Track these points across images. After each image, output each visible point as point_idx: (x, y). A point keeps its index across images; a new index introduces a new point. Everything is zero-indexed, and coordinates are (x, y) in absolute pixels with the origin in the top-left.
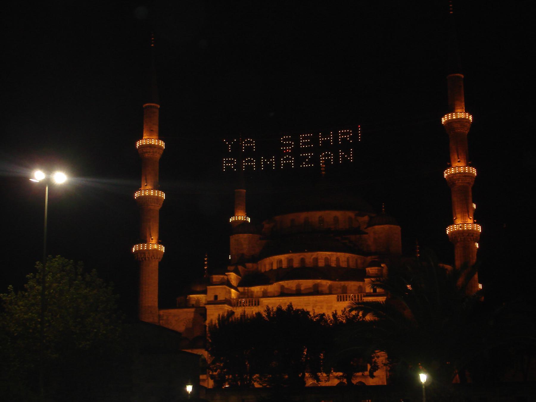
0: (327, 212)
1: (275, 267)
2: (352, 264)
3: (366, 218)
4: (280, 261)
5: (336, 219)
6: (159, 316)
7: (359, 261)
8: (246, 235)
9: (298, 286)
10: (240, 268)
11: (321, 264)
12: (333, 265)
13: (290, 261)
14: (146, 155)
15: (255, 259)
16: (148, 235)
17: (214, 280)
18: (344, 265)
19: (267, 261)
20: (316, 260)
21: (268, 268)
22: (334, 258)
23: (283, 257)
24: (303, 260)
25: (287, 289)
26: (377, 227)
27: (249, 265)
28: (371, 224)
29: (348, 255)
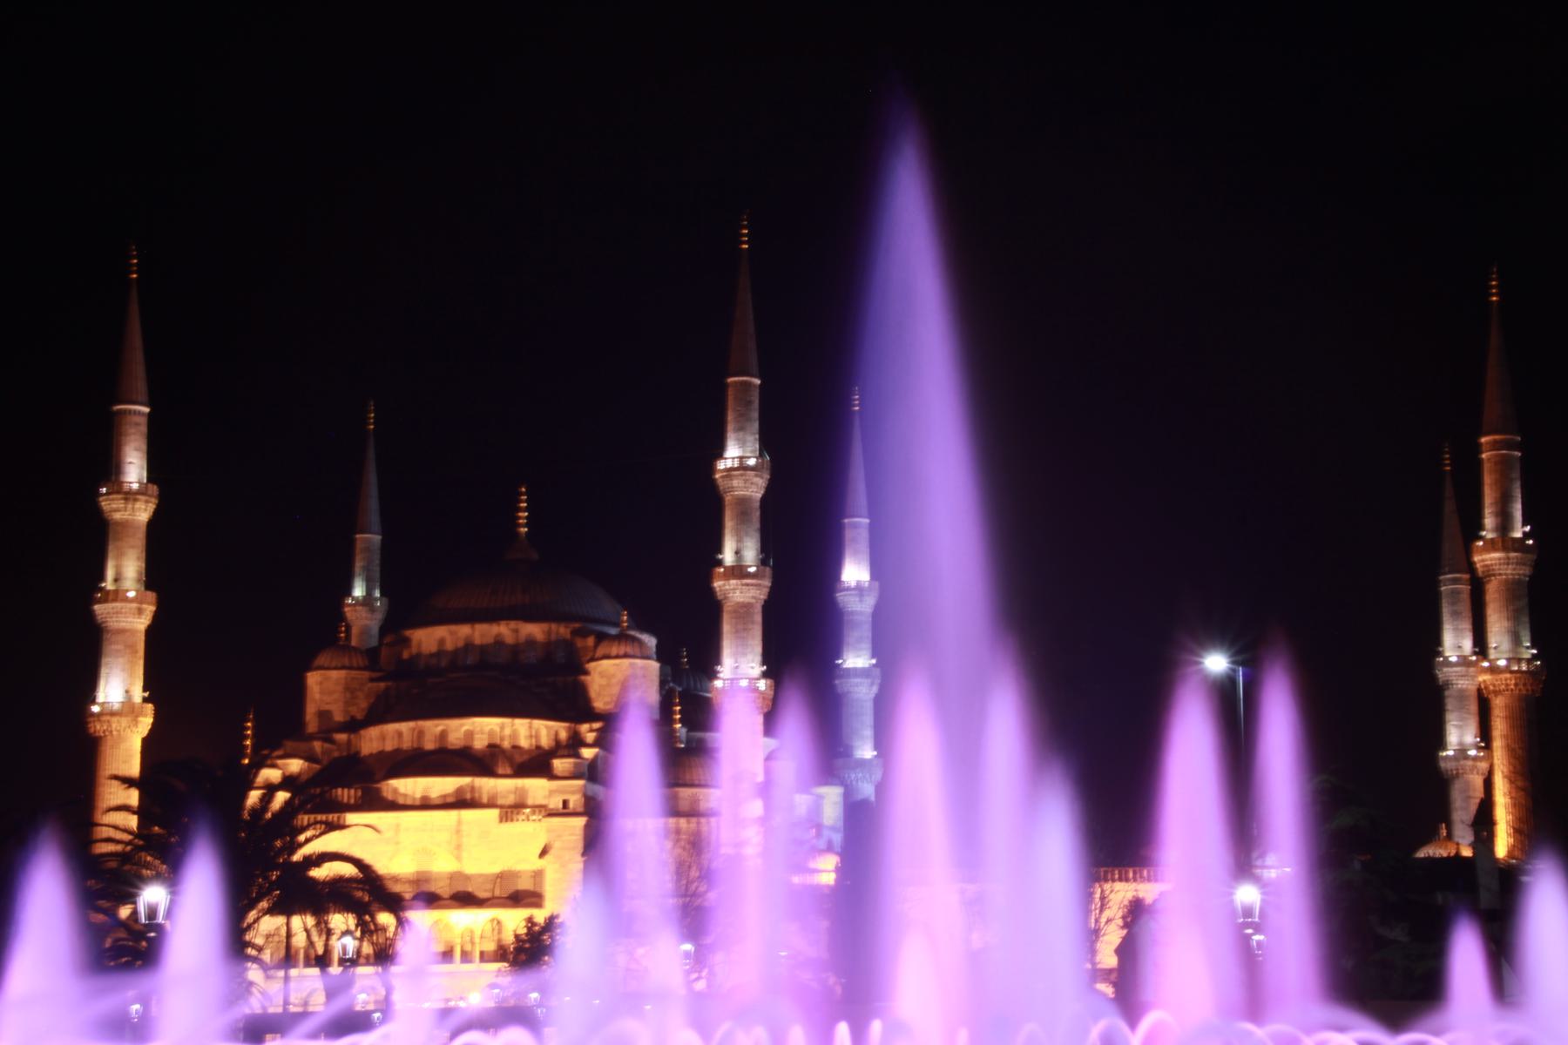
0: (513, 624)
1: (389, 747)
3: (590, 641)
4: (400, 734)
7: (563, 735)
8: (335, 674)
10: (317, 746)
11: (479, 743)
12: (506, 744)
14: (117, 516)
15: (354, 726)
18: (524, 743)
19: (373, 732)
23: (405, 727)
25: (405, 795)
26: (605, 662)
27: (342, 737)
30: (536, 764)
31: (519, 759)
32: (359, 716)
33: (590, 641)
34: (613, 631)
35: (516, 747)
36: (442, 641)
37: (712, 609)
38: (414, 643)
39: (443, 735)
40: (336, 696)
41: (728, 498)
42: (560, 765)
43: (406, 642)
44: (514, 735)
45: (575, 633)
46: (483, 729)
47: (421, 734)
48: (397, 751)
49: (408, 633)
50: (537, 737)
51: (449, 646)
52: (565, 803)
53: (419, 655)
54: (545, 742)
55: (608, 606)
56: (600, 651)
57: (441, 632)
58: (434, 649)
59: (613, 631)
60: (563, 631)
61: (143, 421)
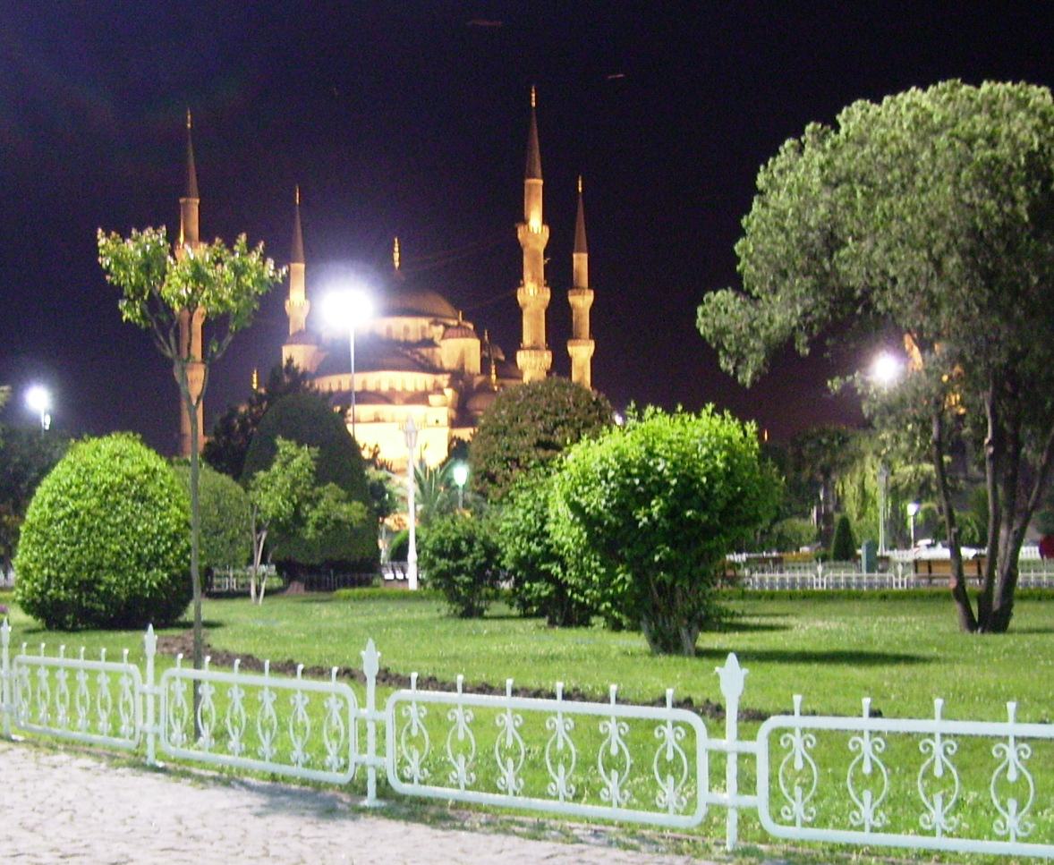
3: (441, 329)
5: (406, 330)
11: (384, 388)
12: (398, 388)
24: (364, 382)
28: (443, 337)
30: (421, 398)
31: (407, 396)
33: (441, 329)
34: (454, 323)
35: (404, 390)
37: (516, 312)
39: (364, 382)
41: (526, 250)
42: (433, 399)
45: (431, 324)
50: (415, 384)
54: (421, 388)
55: (444, 307)
56: (447, 334)
59: (454, 323)
60: (424, 322)
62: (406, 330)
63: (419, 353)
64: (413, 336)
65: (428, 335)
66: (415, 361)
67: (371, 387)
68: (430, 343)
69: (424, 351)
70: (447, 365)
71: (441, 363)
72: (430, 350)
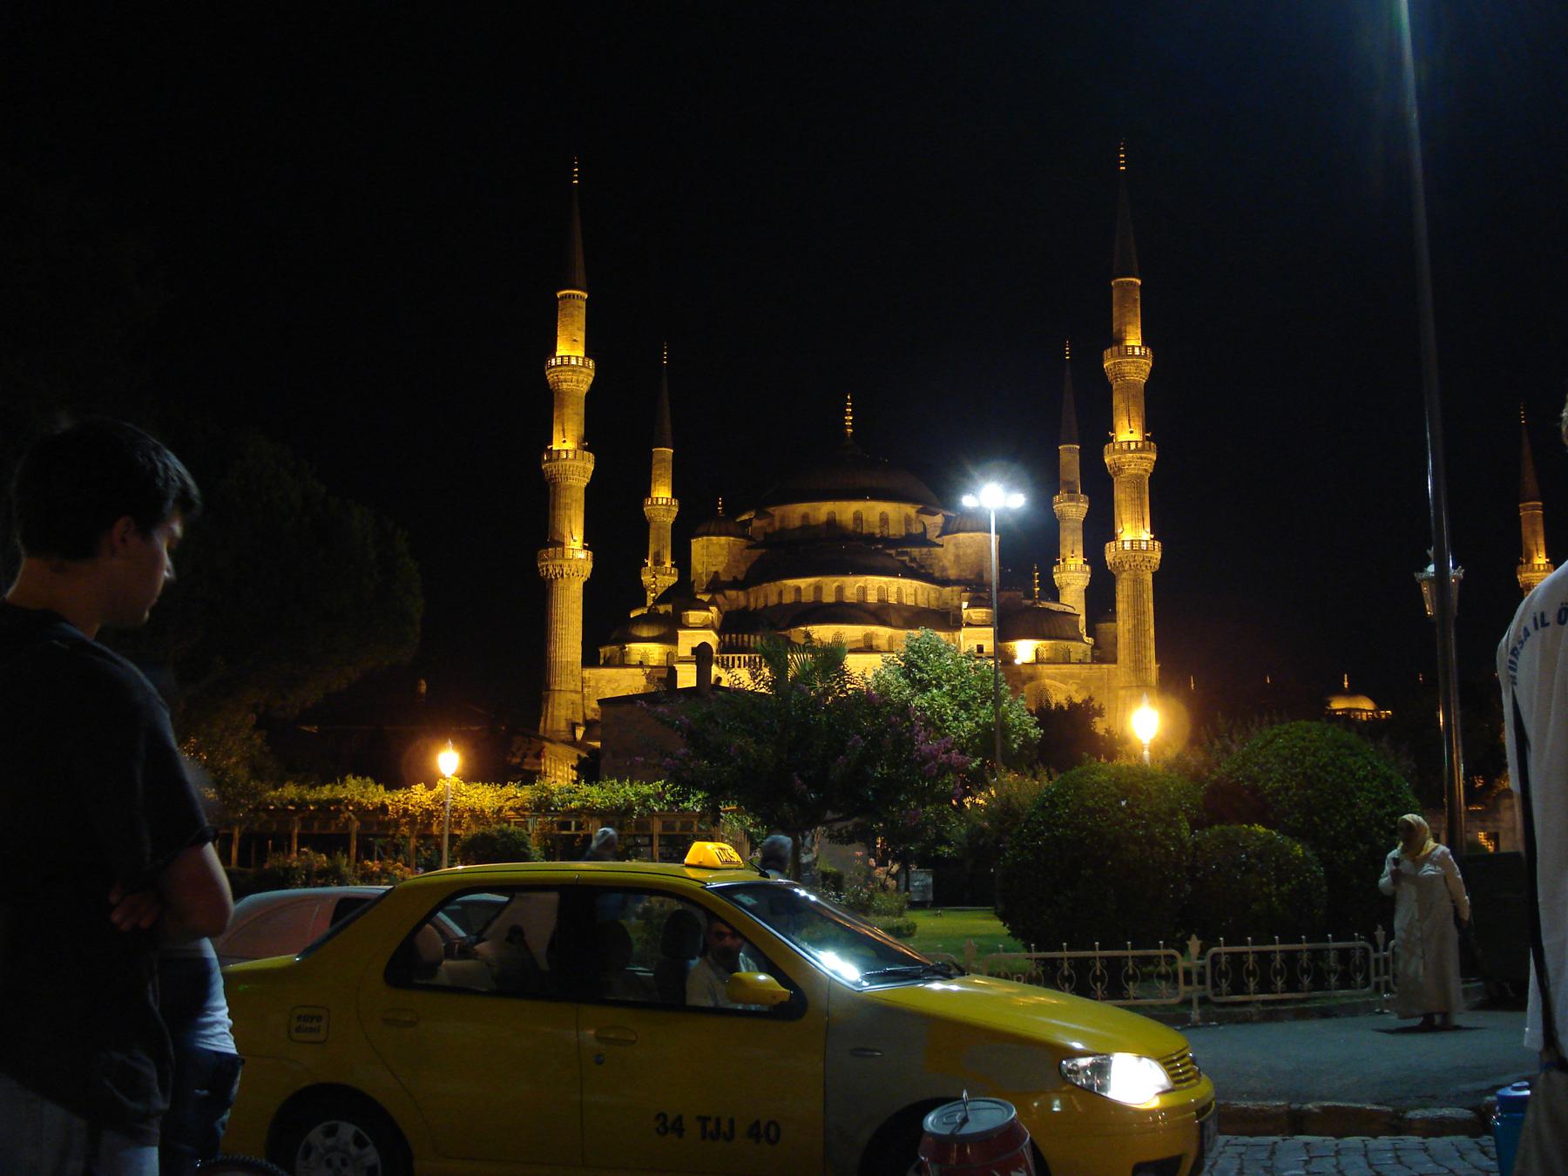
1: (788, 598)
2: (922, 603)
4: (798, 590)
5: (884, 520)
6: (583, 680)
7: (933, 595)
8: (723, 539)
9: (838, 635)
11: (872, 598)
12: (892, 600)
13: (818, 589)
14: (565, 386)
16: (567, 534)
17: (691, 620)
18: (909, 601)
20: (863, 590)
21: (773, 600)
22: (893, 589)
23: (803, 583)
26: (961, 535)
27: (731, 593)
28: (945, 531)
29: (916, 583)
32: (741, 577)
36: (805, 517)
38: (777, 519)
39: (840, 590)
40: (721, 559)
43: (772, 516)
44: (899, 591)
46: (875, 587)
47: (818, 589)
48: (798, 603)
49: (771, 510)
51: (812, 522)
52: (980, 649)
53: (783, 530)
57: (803, 508)
58: (798, 523)
60: (910, 510)
61: (583, 304)
62: (884, 520)
63: (906, 553)
64: (896, 530)
65: (917, 529)
66: (903, 562)
67: (851, 594)
68: (922, 540)
69: (915, 551)
70: (952, 573)
71: (944, 569)
72: (925, 550)
